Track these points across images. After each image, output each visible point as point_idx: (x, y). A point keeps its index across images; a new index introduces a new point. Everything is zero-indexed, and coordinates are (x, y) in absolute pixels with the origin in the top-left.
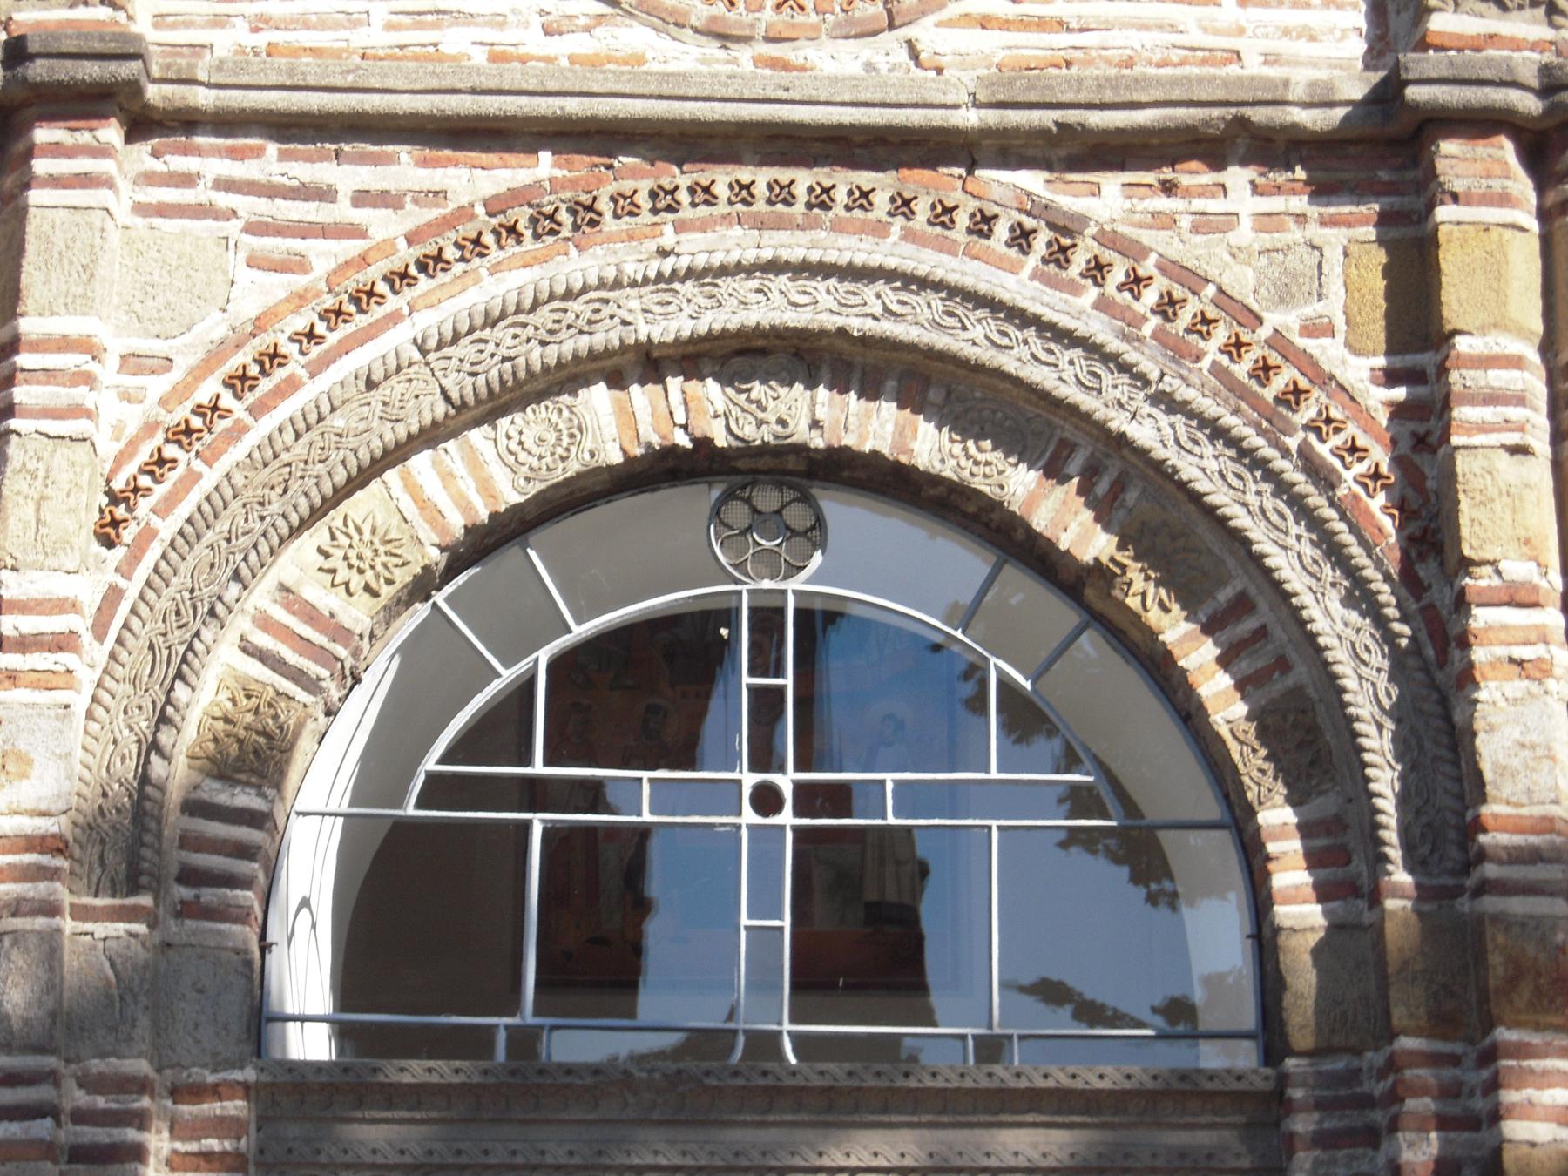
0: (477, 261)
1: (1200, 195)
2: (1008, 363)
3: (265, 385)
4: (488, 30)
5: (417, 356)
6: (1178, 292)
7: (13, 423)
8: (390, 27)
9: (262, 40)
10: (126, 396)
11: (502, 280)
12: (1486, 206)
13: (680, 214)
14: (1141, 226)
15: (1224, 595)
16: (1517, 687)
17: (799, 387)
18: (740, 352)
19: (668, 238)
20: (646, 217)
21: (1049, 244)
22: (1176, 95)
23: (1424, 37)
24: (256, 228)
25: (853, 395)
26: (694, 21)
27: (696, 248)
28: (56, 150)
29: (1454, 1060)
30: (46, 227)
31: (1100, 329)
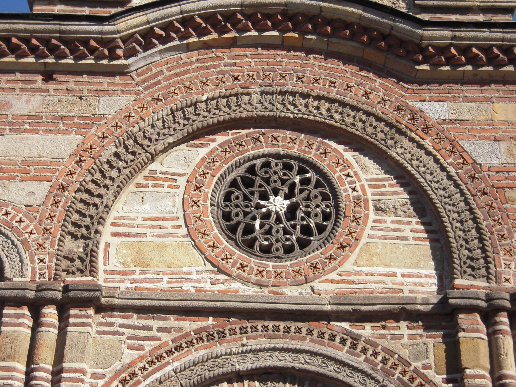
1: (393, 329)
2: (340, 377)
4: (196, 283)
5: (174, 374)
6: (387, 357)
8: (168, 282)
9: (134, 285)
11: (198, 353)
12: (473, 333)
13: (248, 334)
14: (376, 338)
17: (281, 383)
18: (265, 373)
19: (245, 341)
20: (239, 335)
21: (351, 343)
22: (385, 301)
23: (453, 285)
24: (130, 338)
27: (252, 344)
28: (76, 316)
30: (72, 337)
31: (365, 367)
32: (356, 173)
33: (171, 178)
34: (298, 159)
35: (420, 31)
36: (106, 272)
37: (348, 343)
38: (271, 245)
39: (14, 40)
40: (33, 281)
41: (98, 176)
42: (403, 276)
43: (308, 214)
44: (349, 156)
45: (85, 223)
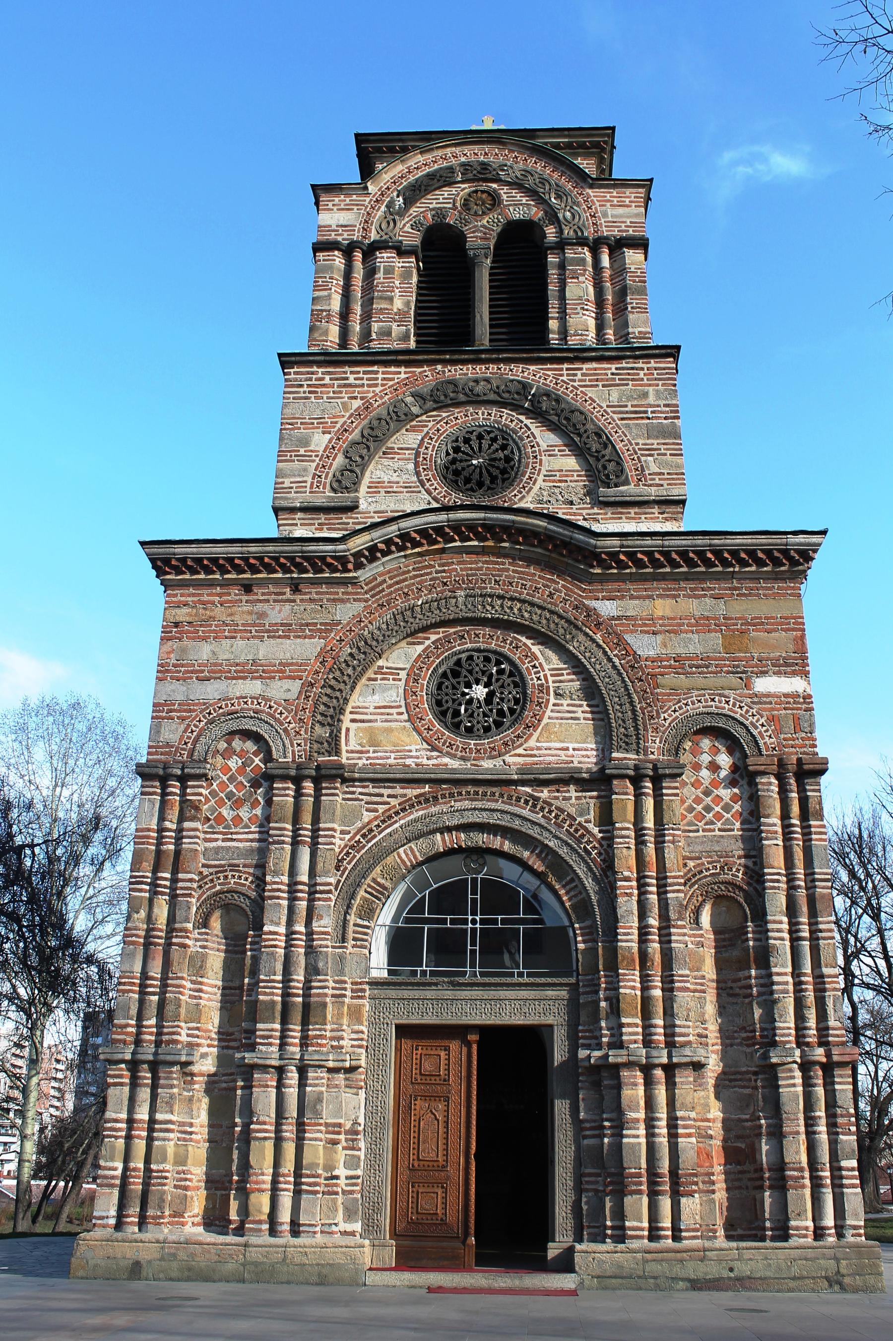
12: (624, 796)
24: (366, 803)
27: (458, 805)
31: (543, 821)
32: (540, 664)
33: (394, 672)
34: (495, 652)
35: (593, 541)
36: (347, 751)
38: (473, 726)
39: (266, 560)
40: (294, 761)
41: (338, 673)
42: (574, 749)
43: (502, 699)
44: (536, 649)
45: (329, 709)
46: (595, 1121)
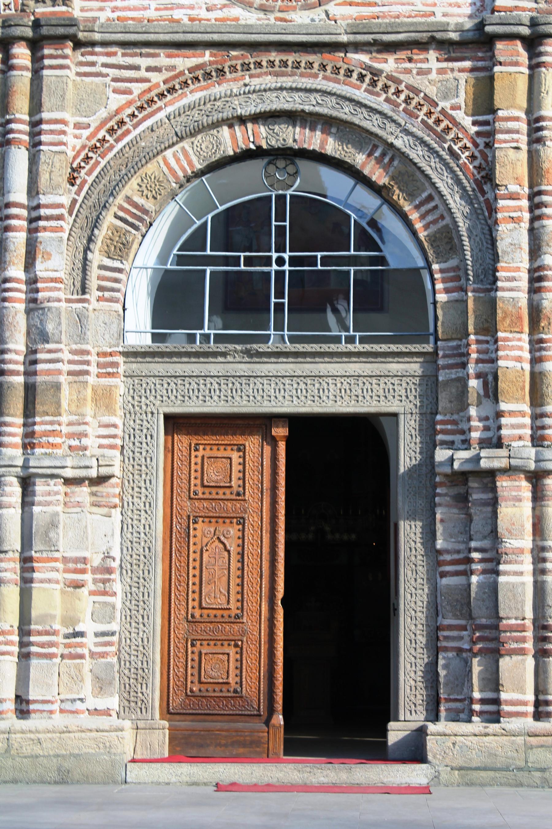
0: (186, 89)
1: (420, 62)
3: (119, 132)
4: (188, 10)
5: (167, 121)
6: (412, 95)
7: (42, 147)
8: (157, 9)
10: (76, 137)
11: (192, 96)
12: (512, 66)
14: (400, 73)
15: (424, 195)
16: (511, 226)
19: (247, 80)
21: (370, 79)
22: (412, 29)
24: (115, 80)
25: (307, 130)
26: (255, 6)
27: (256, 83)
28: (51, 57)
29: (487, 342)
30: (49, 82)
31: (386, 108)
37: (367, 80)
46: (458, 552)
